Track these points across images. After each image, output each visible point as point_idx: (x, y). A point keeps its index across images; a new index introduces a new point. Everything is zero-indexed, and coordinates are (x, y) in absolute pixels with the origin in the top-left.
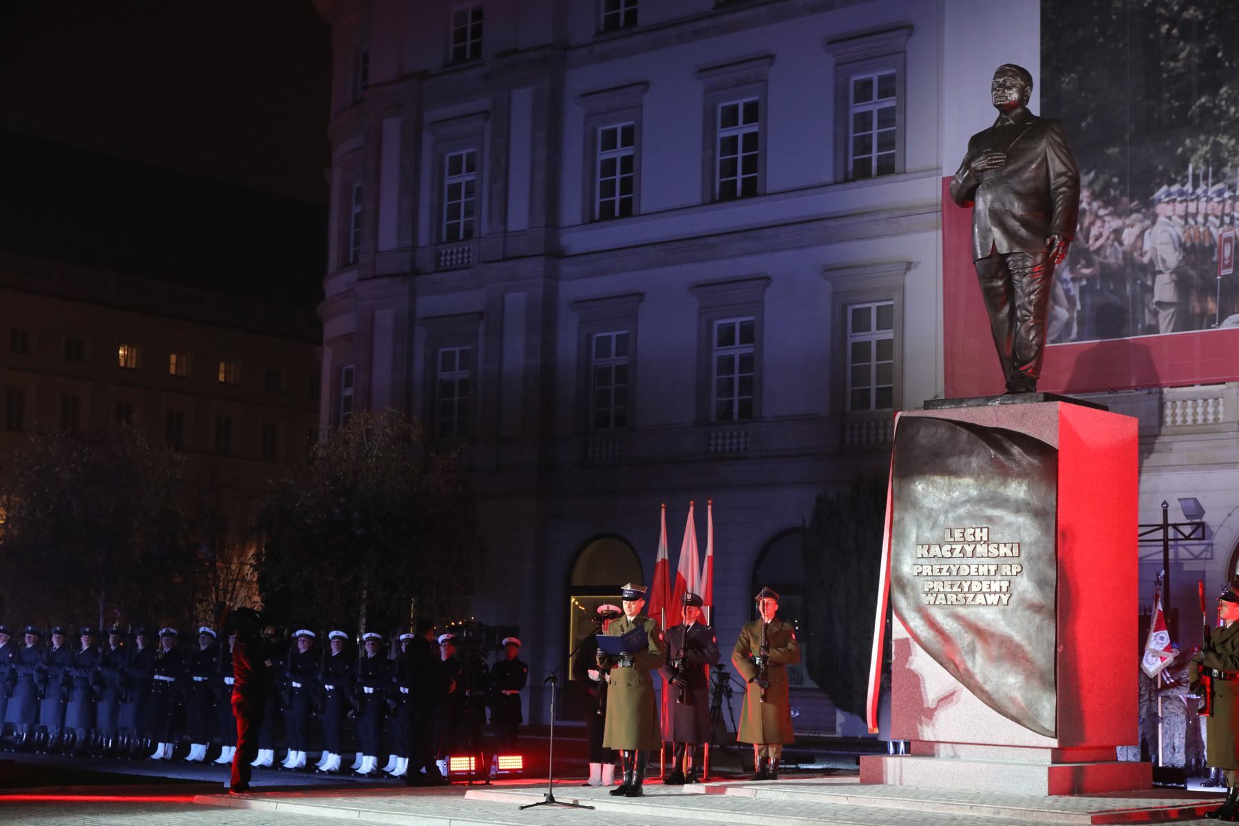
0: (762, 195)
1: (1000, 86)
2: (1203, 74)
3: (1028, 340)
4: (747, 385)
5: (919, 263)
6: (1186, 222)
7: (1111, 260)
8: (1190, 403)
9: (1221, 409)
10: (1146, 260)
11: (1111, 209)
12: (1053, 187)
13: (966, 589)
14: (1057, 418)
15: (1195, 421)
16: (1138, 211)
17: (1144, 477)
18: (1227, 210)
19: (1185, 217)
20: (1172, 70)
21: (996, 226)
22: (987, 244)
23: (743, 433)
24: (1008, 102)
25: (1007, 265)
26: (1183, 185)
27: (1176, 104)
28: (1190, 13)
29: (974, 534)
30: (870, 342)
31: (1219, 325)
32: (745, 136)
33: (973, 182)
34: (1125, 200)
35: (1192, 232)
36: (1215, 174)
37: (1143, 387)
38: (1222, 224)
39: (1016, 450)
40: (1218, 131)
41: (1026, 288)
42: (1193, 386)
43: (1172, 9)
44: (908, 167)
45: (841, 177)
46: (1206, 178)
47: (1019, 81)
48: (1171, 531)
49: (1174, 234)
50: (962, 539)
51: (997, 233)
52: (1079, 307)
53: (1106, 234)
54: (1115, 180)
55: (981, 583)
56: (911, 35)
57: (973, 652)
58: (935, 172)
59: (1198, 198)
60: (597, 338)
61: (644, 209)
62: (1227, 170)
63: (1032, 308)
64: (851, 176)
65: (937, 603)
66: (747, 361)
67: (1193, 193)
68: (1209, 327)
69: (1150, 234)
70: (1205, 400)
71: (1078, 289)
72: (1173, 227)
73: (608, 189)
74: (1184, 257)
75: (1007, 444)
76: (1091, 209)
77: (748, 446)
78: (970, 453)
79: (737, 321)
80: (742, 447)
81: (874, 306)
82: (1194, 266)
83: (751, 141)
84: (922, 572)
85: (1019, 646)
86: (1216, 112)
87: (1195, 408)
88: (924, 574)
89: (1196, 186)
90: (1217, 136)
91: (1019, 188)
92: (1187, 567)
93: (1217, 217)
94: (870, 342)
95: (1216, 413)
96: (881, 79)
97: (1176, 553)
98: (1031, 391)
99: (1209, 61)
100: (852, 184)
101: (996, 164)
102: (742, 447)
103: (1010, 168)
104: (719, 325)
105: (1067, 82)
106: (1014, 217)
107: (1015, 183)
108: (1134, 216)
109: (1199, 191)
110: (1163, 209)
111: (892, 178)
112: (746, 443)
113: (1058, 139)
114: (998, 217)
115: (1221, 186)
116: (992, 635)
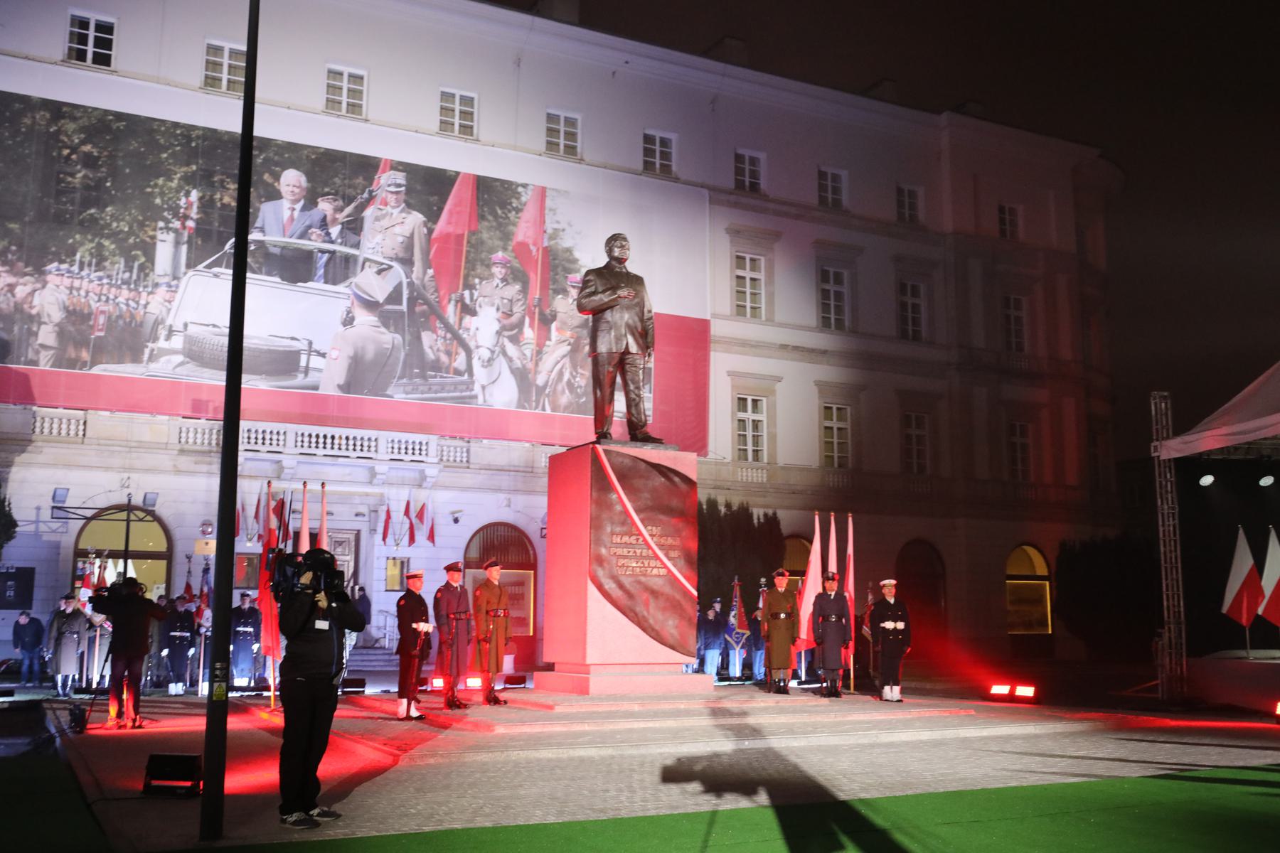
6: (71, 293)
10: (34, 312)
13: (646, 565)
16: (32, 275)
17: (14, 469)
19: (71, 288)
20: (69, 183)
26: (72, 266)
28: (87, 148)
31: (91, 368)
34: (21, 264)
36: (98, 264)
37: (21, 404)
38: (99, 300)
40: (102, 236)
42: (199, 419)
46: (90, 265)
54: (14, 248)
57: (647, 604)
59: (82, 278)
62: (107, 264)
67: (78, 274)
68: (81, 369)
69: (40, 294)
72: (60, 293)
74: (66, 317)
82: (74, 324)
85: (678, 601)
86: (102, 222)
89: (81, 269)
90: (101, 239)
92: (45, 538)
93: (96, 294)
109: (84, 273)
110: (52, 279)
115: (100, 274)
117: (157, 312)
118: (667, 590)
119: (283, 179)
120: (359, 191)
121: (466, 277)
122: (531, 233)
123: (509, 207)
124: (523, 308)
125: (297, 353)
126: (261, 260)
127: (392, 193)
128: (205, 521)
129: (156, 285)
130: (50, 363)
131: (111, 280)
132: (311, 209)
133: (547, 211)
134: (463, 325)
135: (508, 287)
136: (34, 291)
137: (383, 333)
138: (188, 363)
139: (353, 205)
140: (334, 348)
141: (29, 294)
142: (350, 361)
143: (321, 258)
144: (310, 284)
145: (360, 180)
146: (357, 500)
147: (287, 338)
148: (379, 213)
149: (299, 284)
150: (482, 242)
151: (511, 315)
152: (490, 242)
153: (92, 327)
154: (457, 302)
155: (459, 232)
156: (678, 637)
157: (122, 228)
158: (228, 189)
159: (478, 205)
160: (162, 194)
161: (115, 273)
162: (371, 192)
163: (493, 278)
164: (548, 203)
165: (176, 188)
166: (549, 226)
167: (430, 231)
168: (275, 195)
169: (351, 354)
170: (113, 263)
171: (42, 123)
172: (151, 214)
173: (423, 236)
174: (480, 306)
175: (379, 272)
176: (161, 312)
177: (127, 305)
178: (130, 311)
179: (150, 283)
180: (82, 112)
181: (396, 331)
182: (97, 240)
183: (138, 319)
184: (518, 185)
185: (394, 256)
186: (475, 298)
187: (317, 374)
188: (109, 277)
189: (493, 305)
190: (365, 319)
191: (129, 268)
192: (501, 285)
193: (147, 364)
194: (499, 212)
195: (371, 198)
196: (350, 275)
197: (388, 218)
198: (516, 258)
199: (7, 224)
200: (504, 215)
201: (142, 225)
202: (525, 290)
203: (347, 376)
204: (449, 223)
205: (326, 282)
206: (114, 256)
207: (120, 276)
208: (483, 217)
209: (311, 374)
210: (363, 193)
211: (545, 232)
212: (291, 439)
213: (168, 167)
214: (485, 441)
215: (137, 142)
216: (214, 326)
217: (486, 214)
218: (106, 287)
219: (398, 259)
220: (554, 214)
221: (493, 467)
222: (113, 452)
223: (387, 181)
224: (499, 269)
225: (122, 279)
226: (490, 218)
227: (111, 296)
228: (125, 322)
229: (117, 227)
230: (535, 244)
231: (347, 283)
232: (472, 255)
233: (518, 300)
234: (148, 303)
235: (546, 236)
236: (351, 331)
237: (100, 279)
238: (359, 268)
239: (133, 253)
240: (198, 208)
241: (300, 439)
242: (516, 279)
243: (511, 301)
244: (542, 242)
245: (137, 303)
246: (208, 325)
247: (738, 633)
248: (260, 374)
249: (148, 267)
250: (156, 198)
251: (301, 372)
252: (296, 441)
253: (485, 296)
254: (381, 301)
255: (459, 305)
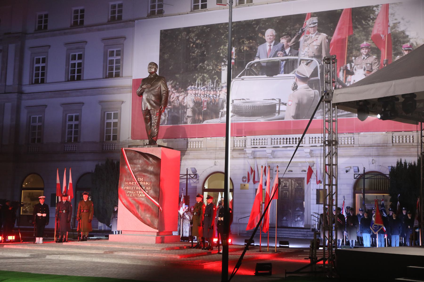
0: (82, 80)
1: (150, 67)
2: (201, 58)
3: (154, 131)
4: (76, 132)
5: (125, 102)
6: (195, 96)
7: (176, 104)
8: (194, 142)
9: (202, 144)
10: (185, 105)
11: (176, 91)
12: (162, 94)
13: (137, 193)
14: (161, 151)
15: (196, 147)
16: (183, 92)
17: (182, 161)
18: (206, 93)
19: (195, 94)
20: (193, 56)
21: (148, 103)
22: (145, 107)
23: (75, 146)
24: (151, 72)
25: (150, 112)
26: (195, 86)
27: (194, 65)
28: (198, 41)
29: (140, 179)
30: (111, 122)
31: (203, 122)
32: (78, 63)
33: (142, 91)
34: (180, 89)
35: (197, 98)
37: (183, 138)
38: (204, 97)
39: (151, 159)
40: (204, 73)
41: (154, 119)
43: (194, 40)
44: (124, 75)
45: (105, 77)
46: (200, 84)
47: (155, 67)
48: (188, 176)
49: (192, 98)
51: (148, 104)
52: (167, 116)
53: (175, 97)
54: (178, 83)
56: (125, 40)
57: (138, 208)
58: (130, 77)
59: (198, 90)
60: (33, 117)
61: (48, 82)
62: (206, 83)
63: (156, 123)
64: (107, 77)
65: (130, 196)
66: (77, 126)
67: (197, 88)
69: (186, 98)
70: (198, 142)
71: (167, 111)
72: (192, 97)
73: (37, 75)
74: (194, 105)
75: (149, 157)
76: (171, 91)
77: (76, 149)
78: (140, 159)
79: (74, 115)
80: (74, 150)
81: (113, 113)
82: (197, 107)
83: (80, 65)
85: (150, 207)
86: (204, 68)
87: (196, 144)
88: (127, 189)
89: (198, 86)
90: (204, 74)
91: (154, 93)
93: (203, 95)
94: (111, 122)
95: (201, 145)
96: (117, 51)
97: (190, 181)
98: (155, 144)
99: (202, 54)
100: (108, 79)
101: (148, 87)
102: (74, 150)
103: (152, 88)
104: (69, 115)
105: (166, 56)
106: (152, 100)
107: (152, 92)
108: (182, 93)
109: (199, 88)
110: (189, 92)
111: (119, 78)
112: (75, 149)
113: (163, 82)
114: (148, 100)
115: (204, 87)
116: (143, 204)
117: (223, 98)
118: (146, 202)
119: (266, 35)
120: (297, 31)
121: (348, 58)
122: (381, 29)
123: (369, 19)
124: (378, 66)
125: (274, 106)
126: (259, 69)
127: (311, 27)
128: (244, 176)
129: (222, 87)
130: (190, 123)
131: (207, 89)
132: (278, 43)
133: (389, 16)
134: (347, 80)
135: (370, 58)
136: (184, 97)
137: (310, 91)
138: (234, 115)
139: (295, 37)
140: (289, 101)
141: (183, 98)
142: (297, 105)
143: (282, 63)
144: (278, 75)
145: (298, 26)
146: (300, 165)
147: (271, 100)
148: (307, 37)
149: (274, 76)
150: (356, 39)
151: (372, 71)
152: (359, 38)
153: (202, 107)
154: (344, 70)
155: (344, 37)
156: (150, 221)
157: (210, 68)
158: (246, 44)
159: (353, 22)
160: (223, 52)
161: (209, 85)
162: (302, 30)
163: (362, 55)
164: (390, 11)
165: (227, 49)
166: (391, 24)
167: (330, 40)
168: (264, 41)
169: (297, 102)
170: (208, 82)
171: (184, 36)
172: (219, 60)
173: (326, 43)
174: (356, 70)
175: (307, 64)
176: (224, 97)
177: (213, 97)
178: (214, 99)
179: (220, 87)
180: (196, 29)
181: (316, 89)
182: (202, 74)
183: (217, 101)
184: (373, 7)
185: (313, 55)
186: (353, 66)
187: (283, 113)
188: (207, 87)
189: (362, 68)
190: (302, 86)
191: (213, 83)
192: (365, 58)
193: (221, 118)
194: (364, 22)
195: (303, 32)
196: (295, 68)
197: (310, 39)
198: (373, 43)
199: (176, 75)
200: (366, 24)
201: (216, 65)
202: (378, 58)
203: (296, 112)
204: (338, 34)
205: (285, 73)
206: (208, 79)
207: (210, 87)
208: (356, 27)
209: (281, 113)
210: (299, 30)
211: (389, 26)
212: (269, 141)
213: (225, 41)
214: (362, 133)
215: (214, 35)
216: (243, 99)
217: (357, 25)
218: (206, 91)
219: (315, 56)
220: (394, 16)
221: (366, 145)
222: (211, 152)
223: (310, 23)
224: (365, 50)
225: (211, 87)
226: (359, 27)
227: (208, 95)
228: (213, 103)
229: (208, 68)
230: (383, 34)
231: (293, 72)
232: (351, 46)
233: (375, 63)
234: (220, 95)
235: (389, 28)
236: (296, 92)
237: (204, 89)
238: (298, 64)
239: (214, 77)
240: (235, 54)
241: (311, 140)
242: (373, 53)
243: (371, 64)
244: (388, 32)
245: (216, 95)
246: (241, 100)
247: (375, 225)
248: (261, 116)
249: (219, 81)
250: (221, 54)
251: (277, 113)
252: (310, 141)
253: (357, 65)
254: (309, 77)
255: (345, 71)
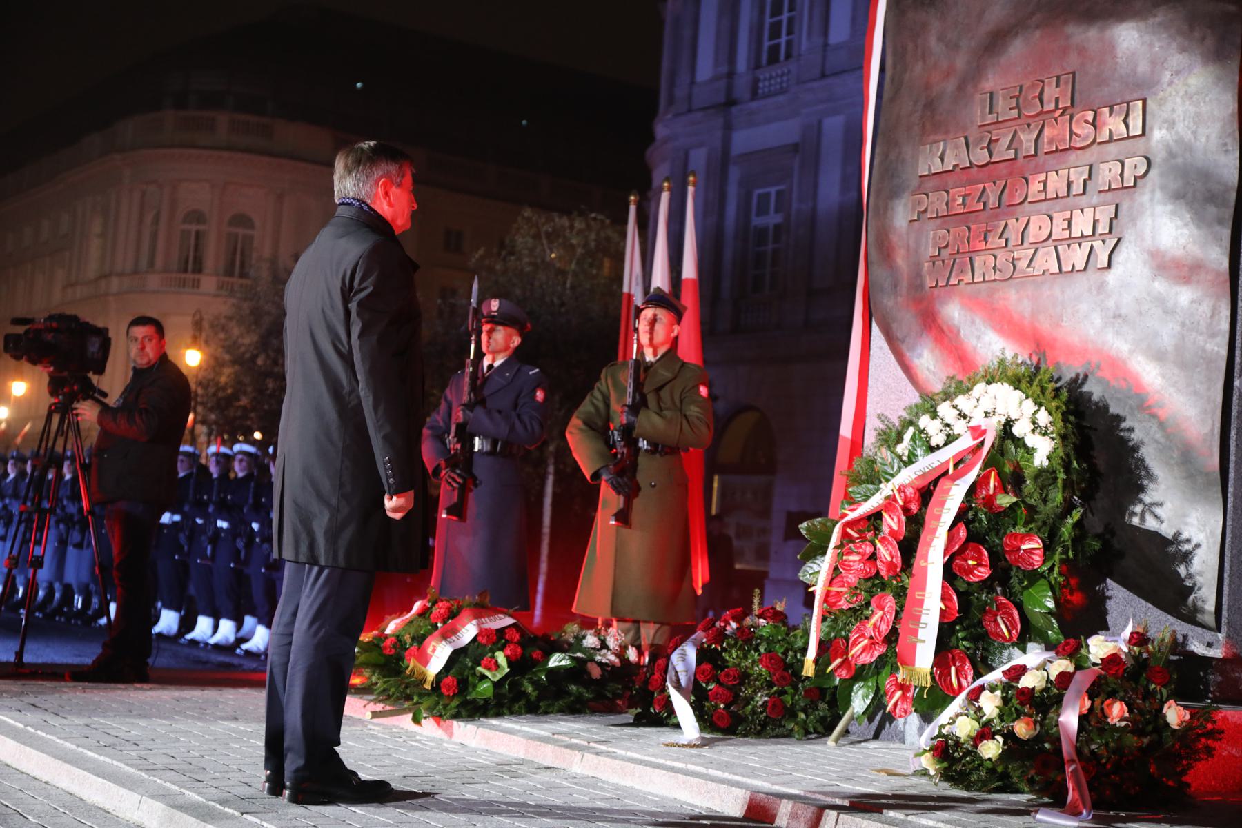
50: (1014, 113)
55: (1051, 219)
84: (925, 211)
